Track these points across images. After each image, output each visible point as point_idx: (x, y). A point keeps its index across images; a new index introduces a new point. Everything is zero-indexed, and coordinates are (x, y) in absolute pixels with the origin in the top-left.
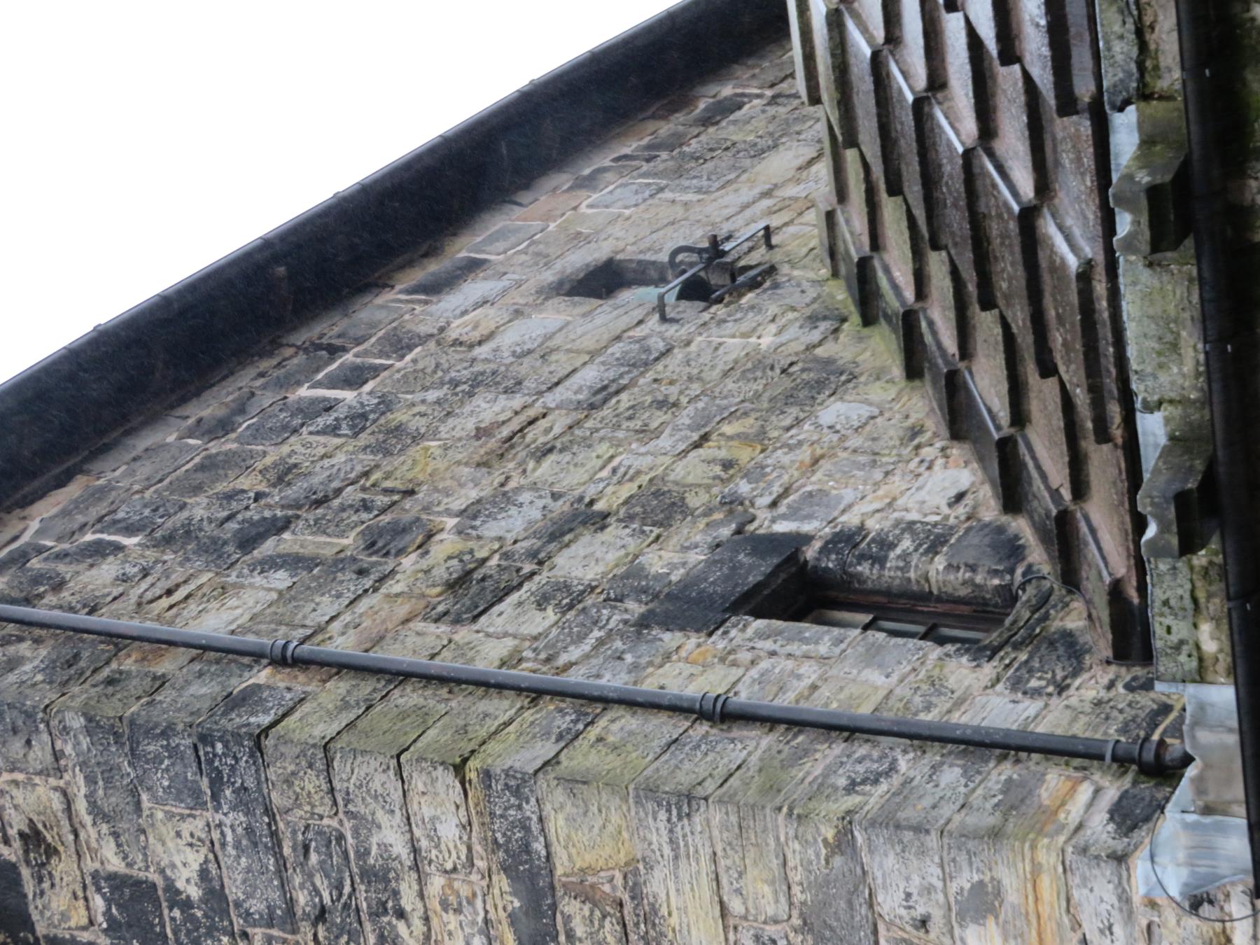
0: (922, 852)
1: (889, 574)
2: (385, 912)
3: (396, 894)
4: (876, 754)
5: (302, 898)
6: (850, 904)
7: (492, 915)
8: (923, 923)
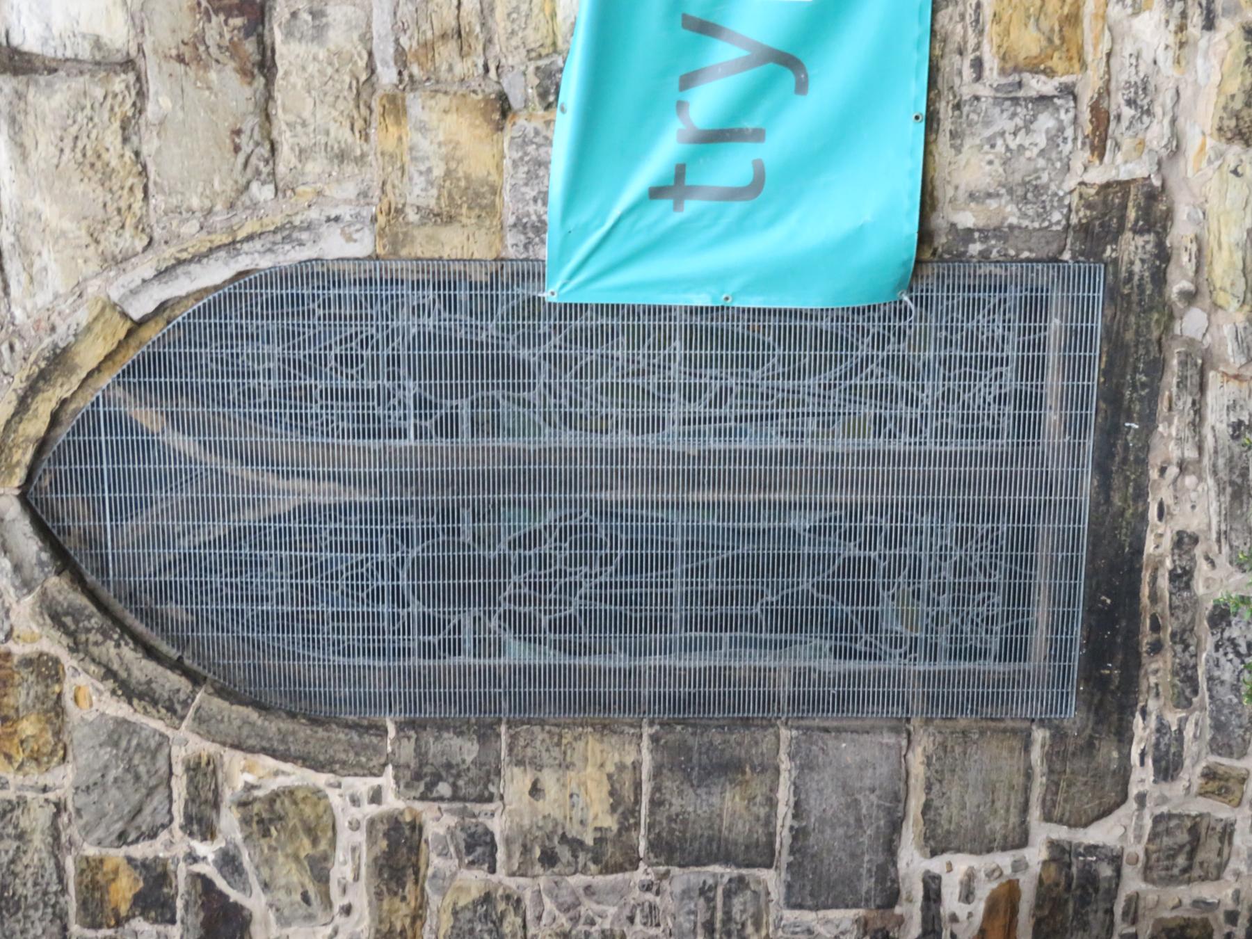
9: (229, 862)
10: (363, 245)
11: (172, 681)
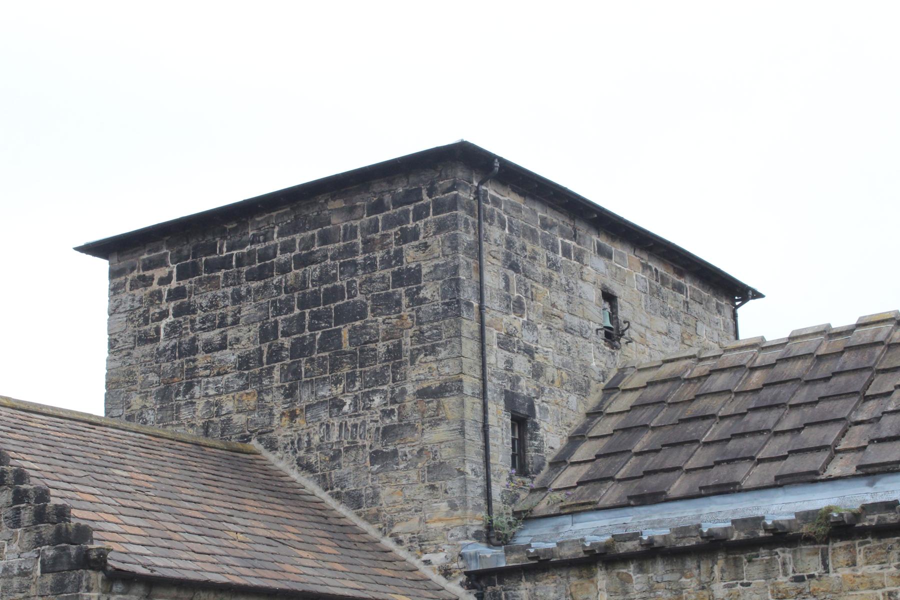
0: (461, 492)
1: (528, 442)
2: (425, 351)
3: (430, 355)
4: (482, 470)
5: (425, 327)
6: (447, 474)
7: (430, 381)
8: (446, 492)
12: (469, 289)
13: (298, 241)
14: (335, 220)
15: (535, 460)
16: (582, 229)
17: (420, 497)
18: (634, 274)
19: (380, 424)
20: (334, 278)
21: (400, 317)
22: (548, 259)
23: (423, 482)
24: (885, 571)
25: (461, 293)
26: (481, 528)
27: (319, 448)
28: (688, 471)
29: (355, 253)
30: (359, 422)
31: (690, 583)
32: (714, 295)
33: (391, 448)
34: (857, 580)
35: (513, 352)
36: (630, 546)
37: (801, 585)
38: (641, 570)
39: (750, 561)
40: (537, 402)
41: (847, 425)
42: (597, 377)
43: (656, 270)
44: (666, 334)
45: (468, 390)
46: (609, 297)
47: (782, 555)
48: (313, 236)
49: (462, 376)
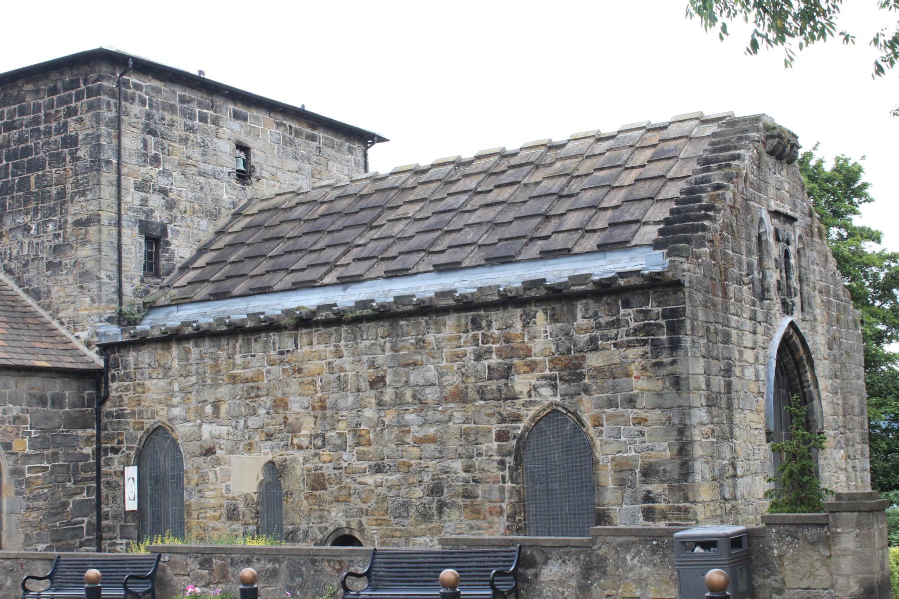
5: (79, 177)
8: (89, 291)
9: (123, 452)
10: (185, 468)
11: (142, 444)
12: (109, 151)
13: (6, 112)
14: (27, 99)
15: (166, 267)
16: (219, 101)
17: (74, 294)
18: (268, 131)
19: (53, 244)
20: (26, 140)
21: (65, 170)
22: (186, 125)
23: (76, 283)
24: (328, 349)
25: (102, 154)
26: (114, 315)
27: (16, 258)
28: (252, 276)
29: (39, 123)
30: (40, 241)
31: (223, 354)
32: (347, 141)
33: (58, 260)
34: (313, 354)
35: (149, 193)
36: (189, 330)
37: (282, 357)
38: (197, 345)
39: (256, 341)
40: (169, 226)
41: (349, 246)
42: (227, 206)
43: (290, 126)
44: (297, 172)
45: (105, 221)
46: (242, 148)
47: (273, 337)
48: (15, 109)
49: (100, 212)
